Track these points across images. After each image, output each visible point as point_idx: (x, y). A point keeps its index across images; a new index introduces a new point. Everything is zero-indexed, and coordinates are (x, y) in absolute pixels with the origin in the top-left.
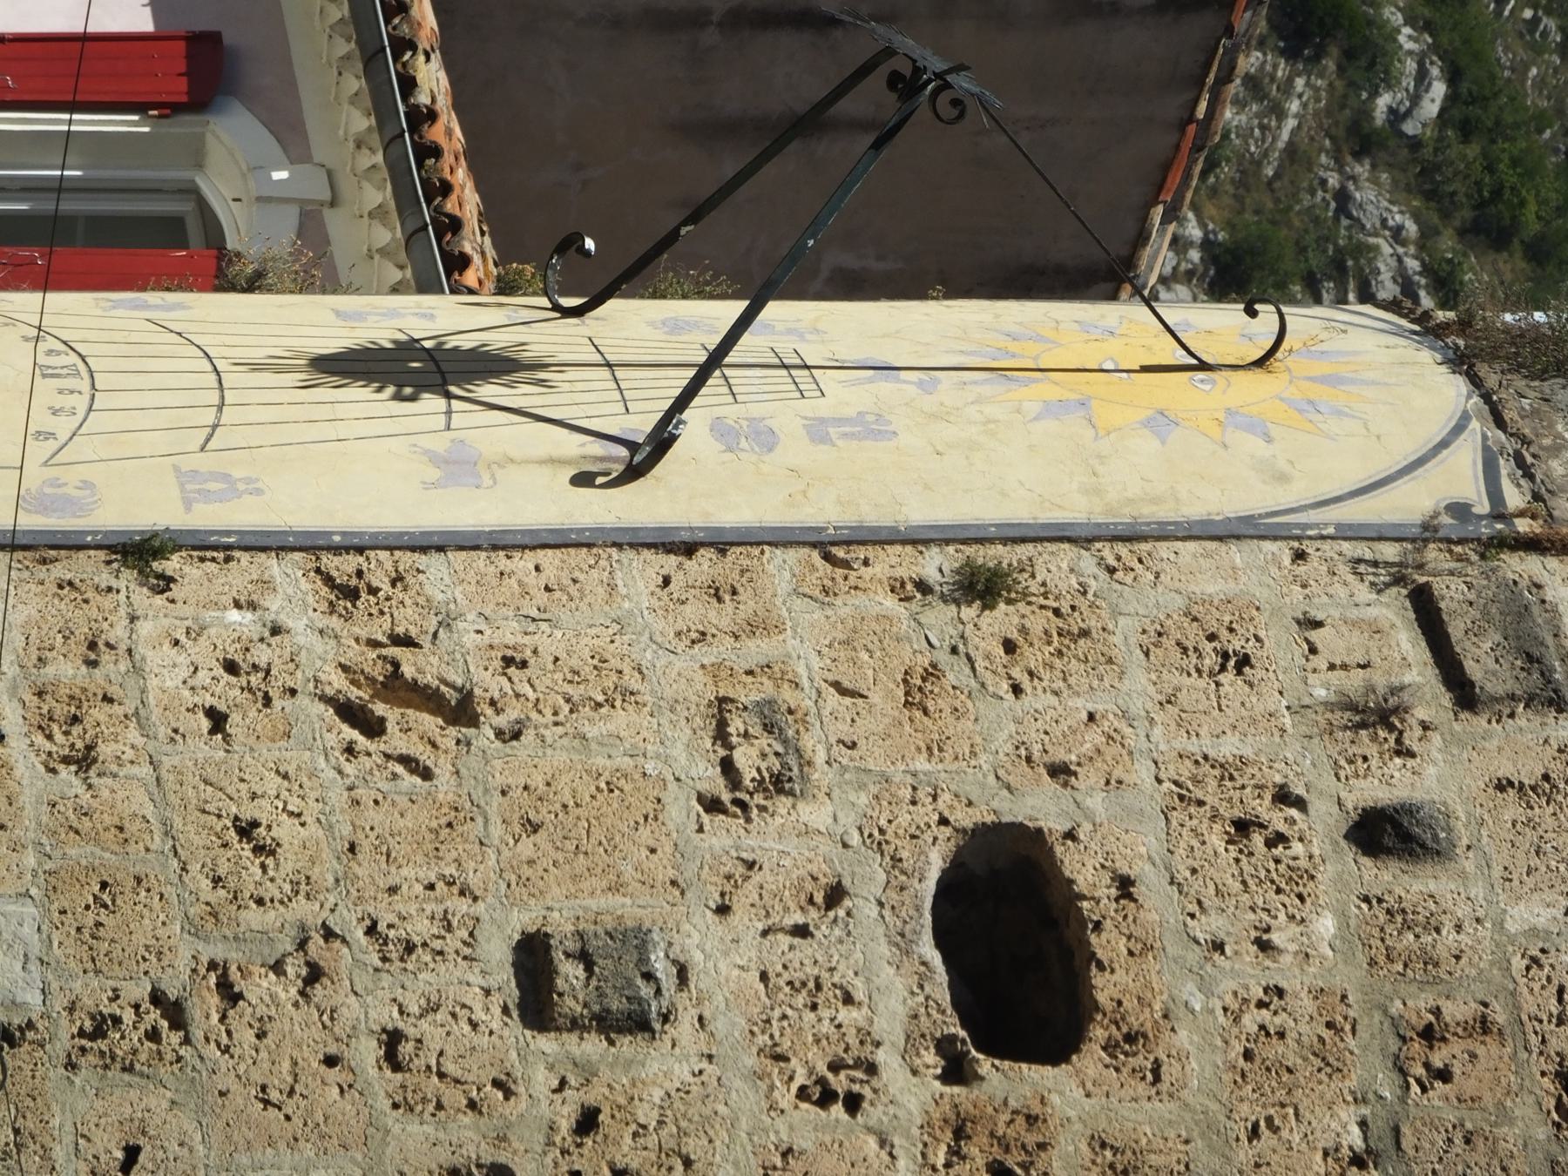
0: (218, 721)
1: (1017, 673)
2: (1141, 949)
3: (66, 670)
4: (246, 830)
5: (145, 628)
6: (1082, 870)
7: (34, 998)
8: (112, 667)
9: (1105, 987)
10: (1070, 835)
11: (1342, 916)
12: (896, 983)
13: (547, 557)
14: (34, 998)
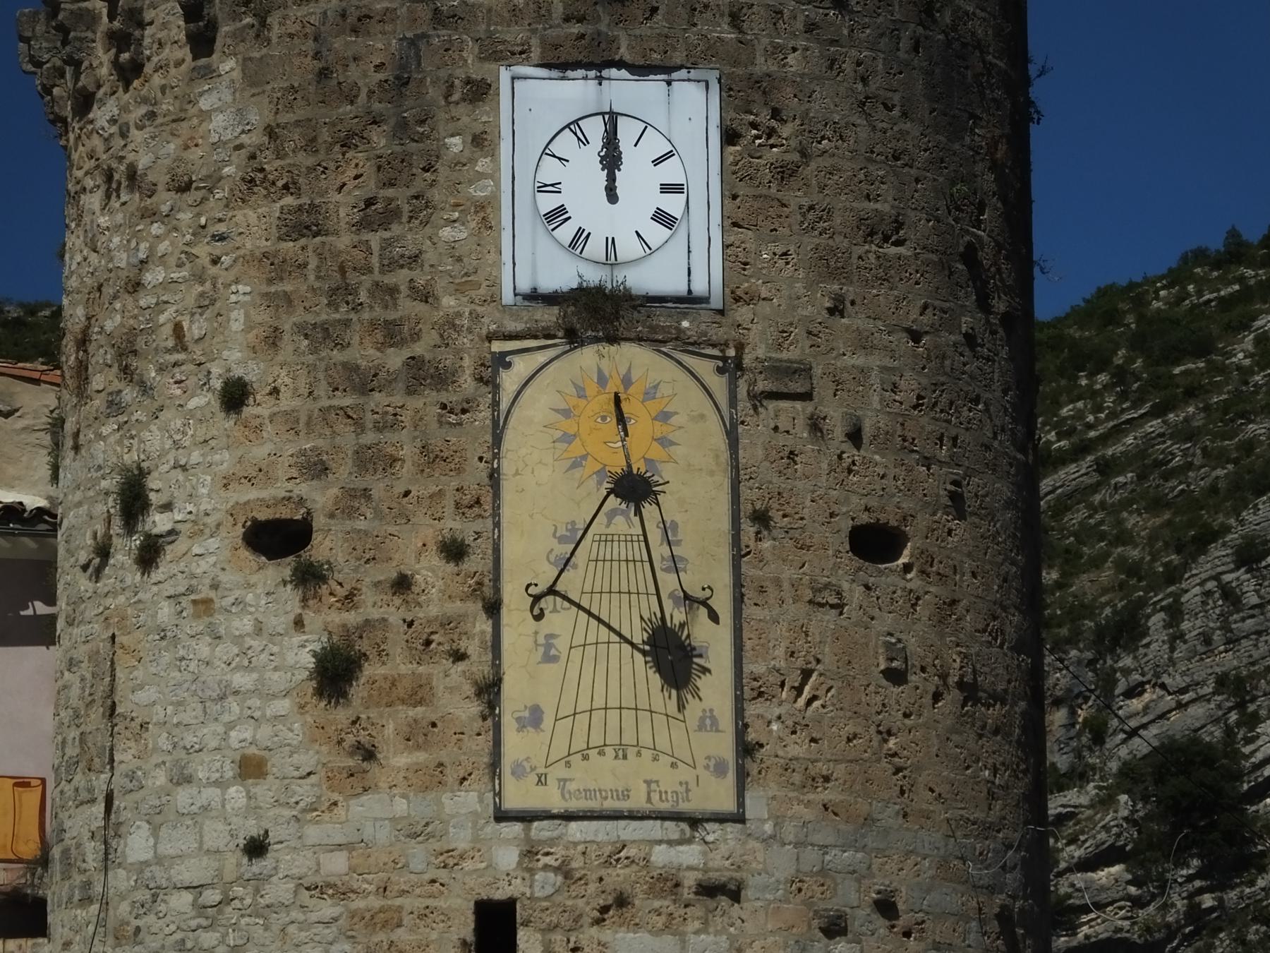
0: (813, 740)
1: (797, 516)
2: (883, 510)
3: (797, 778)
4: (849, 740)
5: (780, 753)
6: (865, 518)
7: (897, 807)
8: (795, 765)
9: (893, 523)
10: (853, 519)
11: (876, 453)
12: (888, 576)
13: (746, 635)
14: (897, 807)
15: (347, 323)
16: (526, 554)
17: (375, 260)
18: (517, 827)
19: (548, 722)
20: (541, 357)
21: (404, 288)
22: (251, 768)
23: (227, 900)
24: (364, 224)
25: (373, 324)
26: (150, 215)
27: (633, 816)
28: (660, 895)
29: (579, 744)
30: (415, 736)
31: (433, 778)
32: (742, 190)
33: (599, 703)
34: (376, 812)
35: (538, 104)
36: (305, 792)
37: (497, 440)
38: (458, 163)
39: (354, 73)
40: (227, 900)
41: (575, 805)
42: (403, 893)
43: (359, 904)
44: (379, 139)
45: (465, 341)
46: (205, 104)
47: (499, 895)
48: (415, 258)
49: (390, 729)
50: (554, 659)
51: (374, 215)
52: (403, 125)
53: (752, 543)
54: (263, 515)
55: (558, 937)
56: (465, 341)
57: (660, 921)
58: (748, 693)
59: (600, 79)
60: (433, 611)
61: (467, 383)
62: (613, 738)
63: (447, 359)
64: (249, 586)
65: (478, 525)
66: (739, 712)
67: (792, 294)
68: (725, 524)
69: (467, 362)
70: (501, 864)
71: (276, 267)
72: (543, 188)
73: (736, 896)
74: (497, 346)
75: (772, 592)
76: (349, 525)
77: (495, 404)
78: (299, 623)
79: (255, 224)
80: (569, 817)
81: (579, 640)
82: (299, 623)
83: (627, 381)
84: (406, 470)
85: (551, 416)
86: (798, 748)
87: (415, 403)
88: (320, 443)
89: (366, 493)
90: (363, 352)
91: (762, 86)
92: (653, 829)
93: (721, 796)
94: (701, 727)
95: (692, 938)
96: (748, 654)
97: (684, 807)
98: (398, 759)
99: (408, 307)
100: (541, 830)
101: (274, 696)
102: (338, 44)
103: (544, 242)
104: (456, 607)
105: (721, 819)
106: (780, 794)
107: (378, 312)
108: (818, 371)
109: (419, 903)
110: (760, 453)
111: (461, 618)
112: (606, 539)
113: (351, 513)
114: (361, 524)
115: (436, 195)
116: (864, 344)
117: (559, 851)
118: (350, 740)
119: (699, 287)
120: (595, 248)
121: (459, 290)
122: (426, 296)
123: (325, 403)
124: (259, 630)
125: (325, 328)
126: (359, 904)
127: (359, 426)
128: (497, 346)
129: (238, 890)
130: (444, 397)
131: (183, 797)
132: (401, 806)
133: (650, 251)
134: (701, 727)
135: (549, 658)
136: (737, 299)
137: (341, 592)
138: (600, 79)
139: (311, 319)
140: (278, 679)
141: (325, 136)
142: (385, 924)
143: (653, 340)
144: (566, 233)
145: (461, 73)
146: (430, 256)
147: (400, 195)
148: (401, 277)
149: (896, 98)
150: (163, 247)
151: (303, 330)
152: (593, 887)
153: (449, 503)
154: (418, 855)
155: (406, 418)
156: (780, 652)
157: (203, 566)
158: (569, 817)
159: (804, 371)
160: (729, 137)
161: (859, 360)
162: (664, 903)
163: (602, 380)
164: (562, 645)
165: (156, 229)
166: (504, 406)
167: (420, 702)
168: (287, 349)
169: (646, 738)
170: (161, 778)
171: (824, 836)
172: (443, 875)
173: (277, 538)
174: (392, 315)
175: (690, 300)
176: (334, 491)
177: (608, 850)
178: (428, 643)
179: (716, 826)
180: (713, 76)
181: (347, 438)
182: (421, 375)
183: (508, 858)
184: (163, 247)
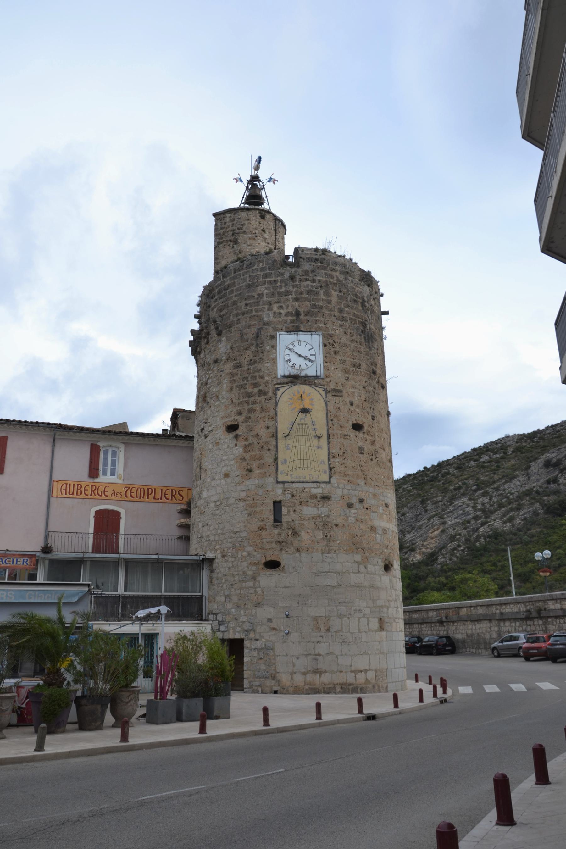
6: (355, 422)
12: (360, 435)
15: (246, 384)
16: (283, 427)
17: (252, 371)
18: (281, 485)
19: (288, 463)
20: (286, 388)
21: (258, 377)
22: (226, 475)
23: (221, 504)
24: (249, 365)
25: (251, 383)
26: (210, 369)
27: (307, 482)
28: (313, 499)
29: (295, 467)
30: (260, 467)
31: (264, 475)
32: (328, 355)
33: (299, 458)
34: (252, 483)
35: (284, 339)
36: (237, 480)
37: (277, 405)
38: (268, 351)
39: (248, 336)
40: (221, 504)
41: (294, 480)
42: (257, 500)
43: (248, 502)
44: (253, 348)
45: (270, 386)
46: (219, 347)
47: (278, 500)
48: (260, 370)
49: (254, 466)
50: (289, 449)
51: (252, 362)
52: (257, 345)
53: (331, 426)
54: (229, 424)
55: (291, 509)
56: (270, 386)
57: (313, 505)
58: (331, 457)
59: (297, 334)
60: (263, 440)
61: (271, 394)
62: (302, 466)
63: (266, 389)
64: (226, 438)
65: (273, 422)
66: (329, 460)
67: (338, 376)
68: (325, 421)
69: (270, 390)
70: (278, 493)
71: (232, 375)
72: (286, 355)
73: (329, 499)
74: (277, 386)
75: (336, 436)
76: (246, 424)
77: (276, 398)
78: (236, 445)
79: (228, 368)
80: (293, 482)
81: (294, 445)
82: (236, 445)
83: (304, 393)
84: (258, 412)
85: (287, 398)
86: (342, 469)
87: (260, 398)
88: (240, 408)
89: (250, 418)
90: (249, 389)
91: (331, 336)
92: (311, 485)
93: (326, 478)
94: (321, 463)
95: (320, 508)
96: (331, 448)
97: (317, 480)
98: (257, 472)
99: (258, 380)
100: (286, 485)
101: (231, 460)
102: (245, 331)
103: (286, 366)
104: (269, 439)
105: (326, 483)
106: (339, 477)
107: (252, 381)
108: (344, 392)
109: (260, 502)
110: (332, 407)
111: (269, 441)
112: (300, 424)
113: (247, 421)
114: (249, 424)
115: (264, 358)
116: (354, 387)
117: (291, 490)
118: (246, 468)
119: (319, 374)
120: (297, 367)
121: (269, 375)
122: (262, 377)
123: (241, 400)
124: (228, 447)
125: (242, 385)
126: (248, 502)
127: (248, 404)
128: (277, 386)
129: (223, 501)
130: (266, 397)
131: (213, 483)
132: (257, 481)
133: (308, 367)
134: (321, 463)
135: (288, 449)
136: (327, 377)
137: (245, 438)
138: (297, 334)
139: (239, 384)
140: (232, 457)
141: (242, 348)
142: (254, 507)
143: (310, 384)
144: (291, 364)
145: (269, 334)
146: (263, 370)
147: (257, 358)
148: (257, 374)
149: (358, 341)
150: (211, 375)
151: (238, 386)
152: (298, 497)
153: (267, 418)
154: (261, 492)
155: (258, 402)
156: (338, 448)
157: (218, 435)
158: (293, 482)
159: (341, 391)
160: (325, 345)
161: (353, 390)
162: (314, 501)
163: (299, 392)
164: (291, 446)
165: (210, 372)
166: (278, 398)
167: (261, 460)
168: (234, 391)
169: (309, 466)
170: (209, 480)
171: (348, 487)
172: (266, 496)
173: (232, 428)
174: (255, 382)
175: (317, 377)
176: (243, 418)
177: (301, 489)
178: (262, 447)
179: (325, 484)
180: (320, 333)
181: (246, 407)
182: (261, 393)
183: (280, 492)
184: (211, 375)
